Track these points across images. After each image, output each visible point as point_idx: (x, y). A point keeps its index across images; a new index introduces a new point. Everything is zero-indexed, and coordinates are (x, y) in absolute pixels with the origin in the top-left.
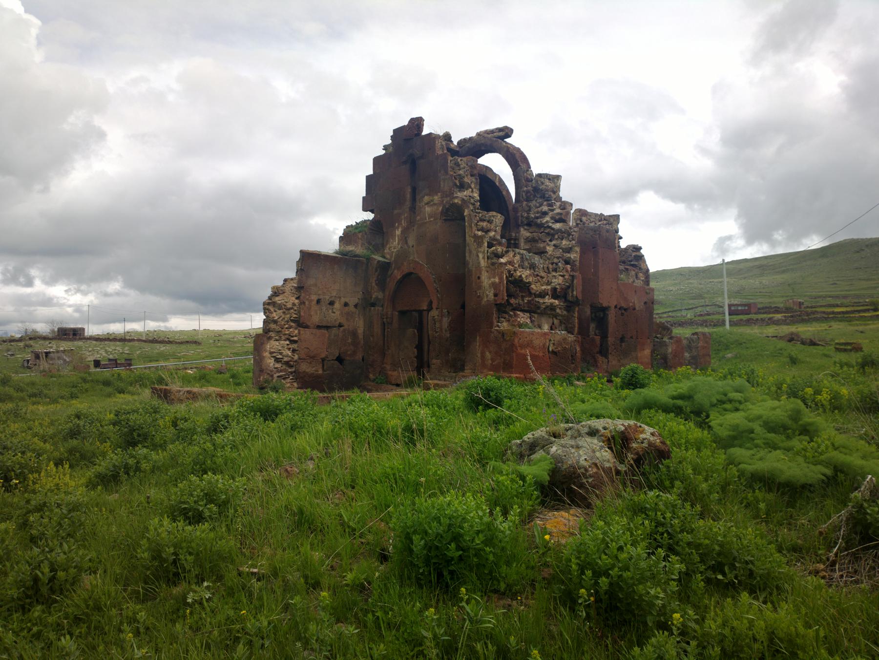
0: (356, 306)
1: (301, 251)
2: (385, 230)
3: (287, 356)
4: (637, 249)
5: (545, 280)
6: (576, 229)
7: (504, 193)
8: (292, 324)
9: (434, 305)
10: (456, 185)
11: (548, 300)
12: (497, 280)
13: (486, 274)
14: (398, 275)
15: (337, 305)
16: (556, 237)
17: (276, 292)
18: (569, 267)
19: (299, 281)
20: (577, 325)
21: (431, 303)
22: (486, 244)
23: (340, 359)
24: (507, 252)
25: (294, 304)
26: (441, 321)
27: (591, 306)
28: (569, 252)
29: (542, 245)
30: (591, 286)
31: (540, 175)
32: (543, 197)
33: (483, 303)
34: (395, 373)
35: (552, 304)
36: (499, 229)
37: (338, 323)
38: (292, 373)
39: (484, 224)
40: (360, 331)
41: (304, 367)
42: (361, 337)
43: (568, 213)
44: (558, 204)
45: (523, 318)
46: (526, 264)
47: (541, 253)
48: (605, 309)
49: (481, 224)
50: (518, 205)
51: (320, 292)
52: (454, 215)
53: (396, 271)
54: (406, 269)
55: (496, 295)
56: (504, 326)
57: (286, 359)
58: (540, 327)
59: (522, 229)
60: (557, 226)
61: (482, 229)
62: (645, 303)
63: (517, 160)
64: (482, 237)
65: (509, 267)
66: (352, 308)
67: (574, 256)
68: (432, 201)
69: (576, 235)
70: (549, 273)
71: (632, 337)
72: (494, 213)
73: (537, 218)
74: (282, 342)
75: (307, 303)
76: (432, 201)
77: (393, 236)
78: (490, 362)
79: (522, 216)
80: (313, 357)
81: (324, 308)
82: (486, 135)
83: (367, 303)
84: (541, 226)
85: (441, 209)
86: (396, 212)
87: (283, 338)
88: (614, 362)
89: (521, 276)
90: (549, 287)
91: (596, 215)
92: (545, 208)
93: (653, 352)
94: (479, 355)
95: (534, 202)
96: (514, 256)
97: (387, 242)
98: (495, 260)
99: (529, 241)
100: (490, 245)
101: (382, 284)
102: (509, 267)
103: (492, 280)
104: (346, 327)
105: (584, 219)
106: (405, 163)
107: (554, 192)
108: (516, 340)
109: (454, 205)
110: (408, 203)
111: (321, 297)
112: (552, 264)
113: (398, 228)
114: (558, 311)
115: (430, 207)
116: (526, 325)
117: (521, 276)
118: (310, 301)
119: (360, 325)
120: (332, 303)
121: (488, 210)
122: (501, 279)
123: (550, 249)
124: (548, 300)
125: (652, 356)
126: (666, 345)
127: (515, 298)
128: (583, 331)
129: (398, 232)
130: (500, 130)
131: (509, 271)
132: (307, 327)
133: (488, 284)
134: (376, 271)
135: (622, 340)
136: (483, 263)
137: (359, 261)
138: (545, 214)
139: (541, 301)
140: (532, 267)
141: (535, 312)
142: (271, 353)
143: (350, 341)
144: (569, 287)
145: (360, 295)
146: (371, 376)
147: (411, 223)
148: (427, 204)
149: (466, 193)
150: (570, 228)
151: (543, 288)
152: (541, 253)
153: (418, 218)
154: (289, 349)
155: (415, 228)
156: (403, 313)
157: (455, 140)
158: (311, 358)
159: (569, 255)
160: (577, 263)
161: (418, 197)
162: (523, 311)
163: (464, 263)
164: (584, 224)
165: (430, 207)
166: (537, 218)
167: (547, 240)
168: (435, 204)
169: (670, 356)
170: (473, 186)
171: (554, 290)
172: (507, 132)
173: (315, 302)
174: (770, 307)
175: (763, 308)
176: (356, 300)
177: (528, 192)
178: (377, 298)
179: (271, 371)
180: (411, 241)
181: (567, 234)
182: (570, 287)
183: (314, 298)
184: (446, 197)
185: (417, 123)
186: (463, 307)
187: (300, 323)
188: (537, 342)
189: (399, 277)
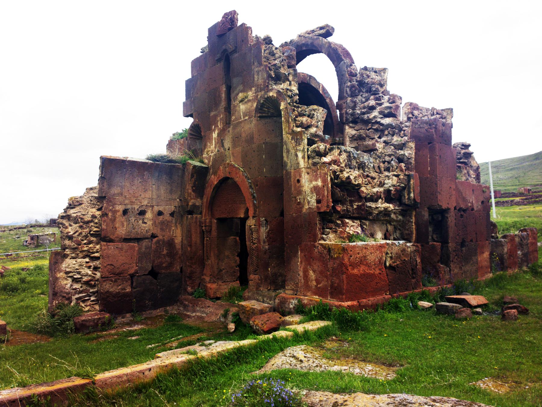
0: (172, 214)
1: (102, 158)
2: (203, 134)
3: (87, 275)
4: (467, 146)
5: (378, 182)
6: (407, 124)
7: (328, 101)
8: (92, 239)
9: (251, 213)
10: (272, 78)
11: (382, 205)
12: (319, 183)
13: (307, 176)
14: (214, 180)
15: (149, 215)
16: (386, 133)
17: (73, 204)
18: (403, 165)
19: (101, 190)
20: (414, 232)
21: (247, 211)
22: (306, 141)
23: (153, 273)
24: (331, 150)
25: (94, 217)
26: (258, 231)
27: (428, 208)
28: (402, 149)
29: (370, 143)
30: (429, 186)
31: (365, 69)
32: (369, 91)
33: (304, 211)
34: (214, 286)
35: (386, 209)
36: (321, 125)
37: (150, 234)
38: (94, 293)
39: (304, 119)
40: (178, 240)
41: (108, 287)
42: (178, 246)
43: (398, 107)
44: (386, 98)
45: (353, 227)
46: (354, 163)
47: (371, 150)
48: (443, 212)
49: (300, 119)
50: (341, 102)
51: (127, 202)
52: (269, 110)
53: (213, 176)
54: (222, 174)
55: (318, 201)
56: (331, 239)
57: (85, 279)
58: (372, 235)
59: (347, 127)
60: (387, 121)
61: (301, 125)
62: (483, 202)
63: (338, 56)
64: (300, 133)
65: (334, 167)
66: (167, 217)
67: (409, 152)
68: (246, 97)
69: (408, 130)
70: (381, 172)
71: (471, 241)
72: (315, 107)
73: (364, 113)
74: (79, 260)
75: (110, 214)
76: (246, 97)
77: (210, 139)
78: (314, 283)
79: (347, 113)
80: (119, 274)
81: (133, 219)
82: (307, 35)
83: (185, 211)
84: (367, 122)
85: (255, 105)
86: (212, 114)
87: (81, 255)
88: (456, 271)
89: (348, 178)
90: (381, 189)
91: (427, 110)
92: (372, 103)
93: (491, 254)
94: (301, 274)
95: (359, 97)
96: (340, 154)
97: (205, 146)
98: (316, 160)
99: (355, 140)
100: (311, 142)
101: (199, 190)
102: (334, 167)
104: (161, 237)
105: (416, 113)
106: (219, 60)
107: (382, 86)
108: (346, 259)
109: (270, 98)
110: (223, 104)
111: (129, 207)
112: (384, 162)
113: (214, 130)
114: (393, 216)
115: (245, 105)
116: (356, 237)
117: (348, 178)
118: (115, 212)
119: (177, 235)
120: (142, 213)
121: (308, 105)
122: (324, 181)
123: (380, 146)
124: (382, 205)
125: (491, 258)
126: (502, 246)
127: (343, 204)
128: (421, 239)
129: (215, 135)
130: (321, 28)
131: (334, 172)
132: (111, 241)
133: (309, 187)
134: (192, 176)
135: (463, 244)
136: (302, 164)
137: (174, 166)
138: (372, 108)
139: (373, 205)
140: (362, 166)
141: (366, 219)
142: (67, 273)
143: (165, 252)
144: (404, 188)
145: (177, 202)
146: (189, 289)
147: (227, 123)
148: (241, 101)
149: (284, 86)
150: (401, 123)
151: (375, 190)
152: (371, 150)
153: (233, 117)
154: (89, 267)
155: (230, 129)
156: (221, 221)
157: (277, 43)
158: (115, 275)
159: (402, 152)
160: (413, 161)
161: (233, 95)
162: (353, 218)
163: (282, 165)
164: (416, 117)
165: (245, 105)
166: (364, 113)
167: (376, 137)
168: (249, 101)
169: (506, 256)
170: (291, 78)
171: (388, 191)
172: (328, 32)
173: (121, 212)
174: (509, 193)
175: (504, 194)
176: (173, 208)
177: (352, 86)
178: (194, 205)
179: (68, 293)
180: (228, 144)
181: (397, 129)
182: (407, 187)
183: (120, 208)
185: (230, 19)
186: (282, 214)
187: (101, 237)
188: (372, 258)
189: (216, 183)
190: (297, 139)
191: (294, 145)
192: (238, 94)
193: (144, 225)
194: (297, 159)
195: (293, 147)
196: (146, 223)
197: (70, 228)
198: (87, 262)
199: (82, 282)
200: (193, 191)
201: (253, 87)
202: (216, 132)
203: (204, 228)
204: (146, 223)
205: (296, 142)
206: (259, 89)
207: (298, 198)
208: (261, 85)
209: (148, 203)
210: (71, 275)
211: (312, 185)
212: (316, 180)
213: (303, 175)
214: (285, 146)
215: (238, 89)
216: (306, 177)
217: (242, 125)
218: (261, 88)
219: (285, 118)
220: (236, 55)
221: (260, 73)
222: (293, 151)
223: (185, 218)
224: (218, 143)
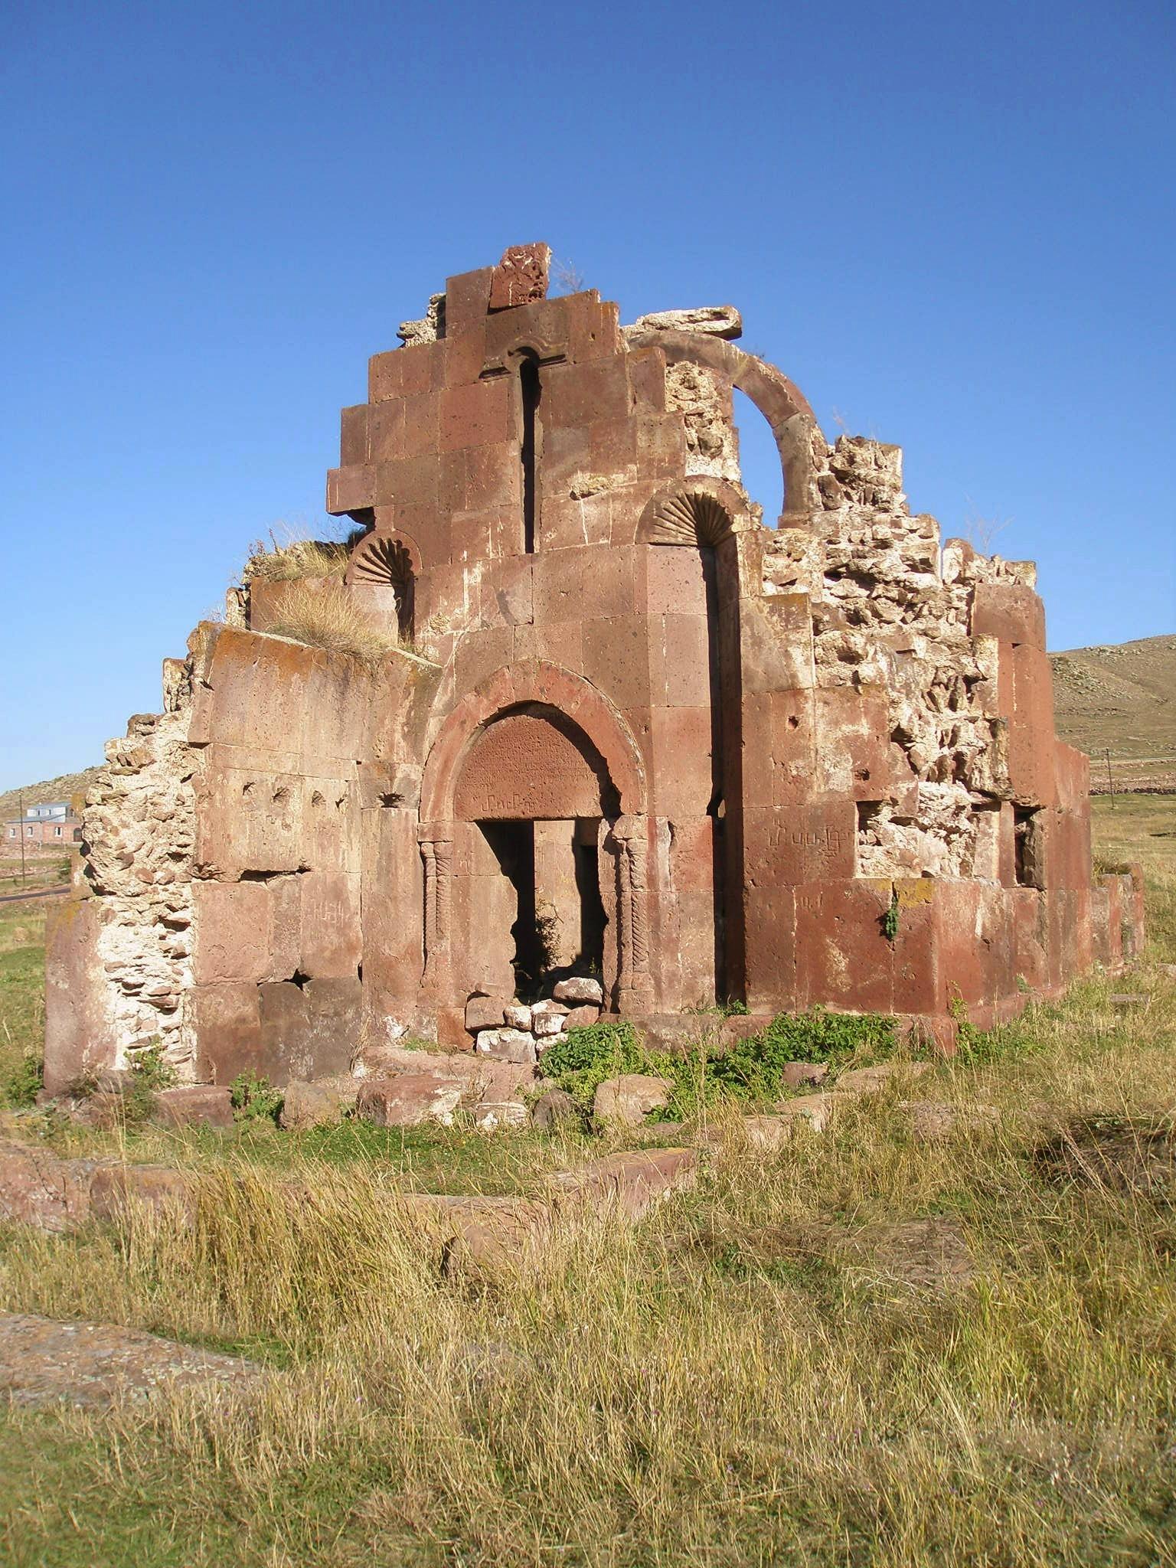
12: (864, 728)
13: (821, 709)
15: (296, 804)
25: (181, 801)
33: (812, 798)
40: (353, 884)
75: (218, 796)
77: (453, 591)
85: (639, 511)
86: (458, 517)
103: (847, 728)
111: (256, 777)
113: (470, 564)
123: (920, 644)
129: (473, 577)
168: (615, 497)
176: (343, 787)
180: (524, 603)
184: (663, 474)
190: (789, 614)
191: (778, 628)
192: (570, 474)
193: (285, 833)
194: (788, 666)
195: (776, 633)
196: (287, 826)
197: (124, 832)
198: (162, 938)
199: (144, 997)
200: (405, 736)
201: (632, 461)
202: (478, 570)
203: (428, 849)
204: (287, 826)
205: (787, 621)
206: (653, 468)
207: (792, 765)
208: (662, 460)
209: (294, 768)
210: (119, 973)
211: (839, 734)
212: (853, 720)
213: (809, 706)
214: (745, 631)
215: (570, 460)
216: (819, 712)
217: (588, 558)
218: (659, 469)
219: (749, 557)
220: (559, 368)
221: (659, 432)
222: (774, 644)
223: (376, 814)
224: (483, 602)
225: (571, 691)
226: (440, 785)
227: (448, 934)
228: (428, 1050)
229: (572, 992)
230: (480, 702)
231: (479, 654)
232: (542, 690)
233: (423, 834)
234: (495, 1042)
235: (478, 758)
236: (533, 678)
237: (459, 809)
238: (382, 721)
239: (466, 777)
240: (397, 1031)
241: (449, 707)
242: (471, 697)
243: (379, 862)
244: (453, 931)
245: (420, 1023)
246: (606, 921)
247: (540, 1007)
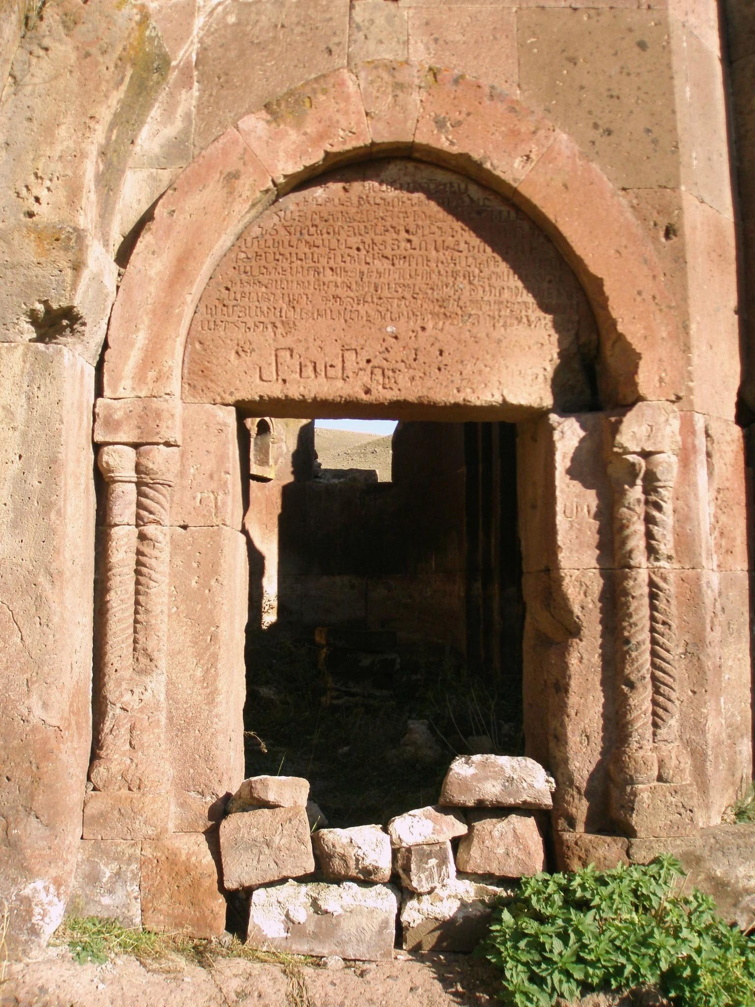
225: (514, 133)
226: (164, 312)
227: (162, 662)
228: (137, 952)
229: (491, 791)
230: (277, 136)
231: (260, 46)
232: (440, 124)
233: (111, 424)
234: (302, 914)
235: (254, 259)
236: (416, 97)
237: (199, 376)
238: (49, 129)
239: (219, 303)
240: (52, 915)
241: (177, 150)
242: (255, 124)
243: (22, 477)
244: (172, 655)
245: (93, 878)
246: (574, 630)
247: (417, 826)
